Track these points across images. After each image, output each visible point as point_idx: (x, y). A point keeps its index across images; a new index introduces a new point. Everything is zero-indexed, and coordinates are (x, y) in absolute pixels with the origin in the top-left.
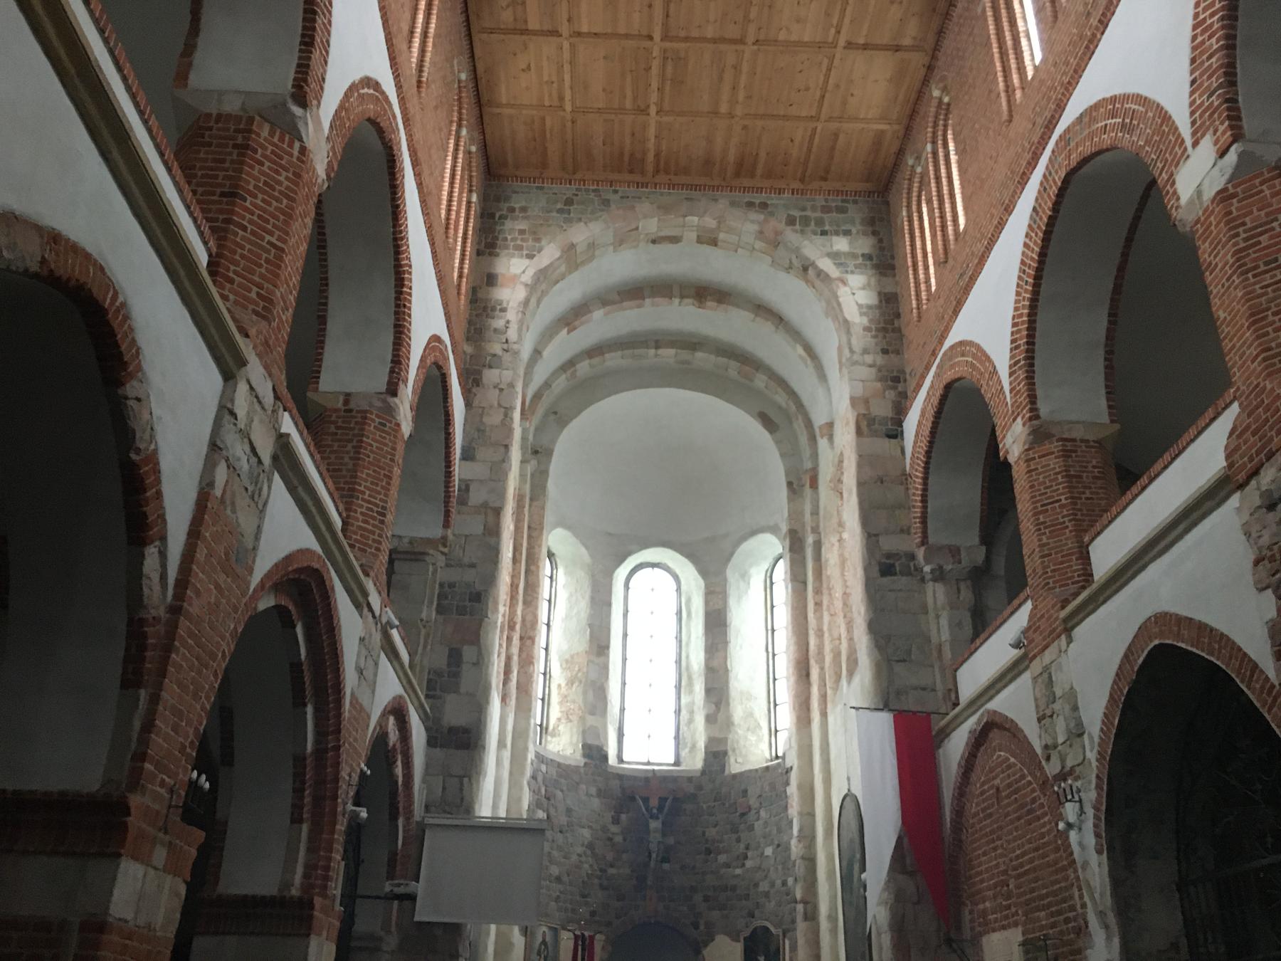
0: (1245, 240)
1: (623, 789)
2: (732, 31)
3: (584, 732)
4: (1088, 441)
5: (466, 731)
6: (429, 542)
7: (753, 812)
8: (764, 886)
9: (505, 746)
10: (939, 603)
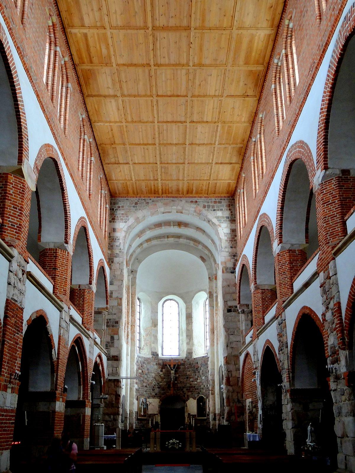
0: (281, 266)
1: (163, 362)
2: (182, 161)
3: (151, 348)
4: (268, 290)
5: (117, 356)
6: (103, 309)
7: (199, 368)
8: (202, 387)
9: (128, 355)
10: (243, 320)
